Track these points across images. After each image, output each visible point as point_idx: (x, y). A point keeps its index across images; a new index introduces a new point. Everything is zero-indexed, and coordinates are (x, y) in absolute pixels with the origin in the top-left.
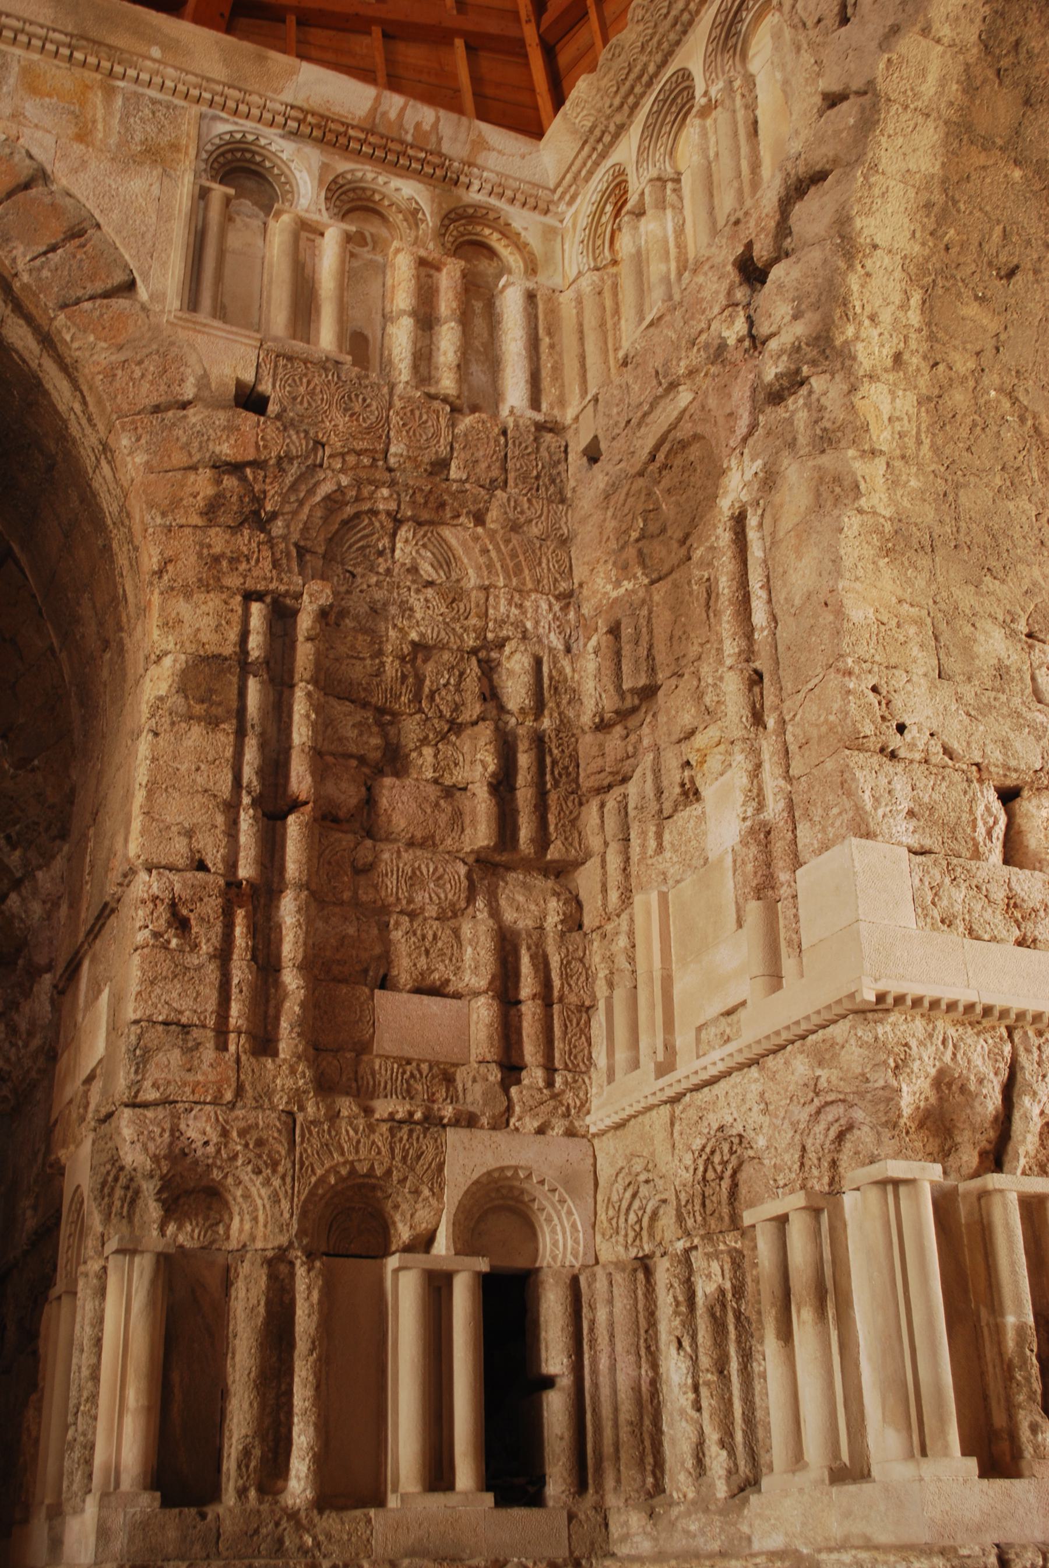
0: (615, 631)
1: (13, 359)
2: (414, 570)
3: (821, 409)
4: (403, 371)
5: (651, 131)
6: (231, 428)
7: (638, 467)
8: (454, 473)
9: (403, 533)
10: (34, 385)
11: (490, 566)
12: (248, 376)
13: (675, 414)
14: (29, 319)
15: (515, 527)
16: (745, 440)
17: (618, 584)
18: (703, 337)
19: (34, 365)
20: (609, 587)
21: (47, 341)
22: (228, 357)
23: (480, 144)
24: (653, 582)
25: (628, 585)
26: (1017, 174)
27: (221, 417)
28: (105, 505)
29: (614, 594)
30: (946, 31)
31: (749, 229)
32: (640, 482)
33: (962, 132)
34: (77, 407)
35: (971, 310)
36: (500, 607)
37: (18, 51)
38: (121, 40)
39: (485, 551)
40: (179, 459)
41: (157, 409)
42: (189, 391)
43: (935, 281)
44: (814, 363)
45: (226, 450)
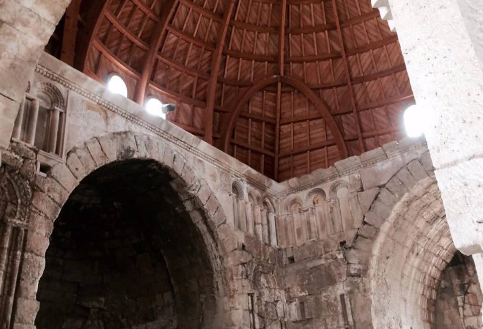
0: (302, 303)
1: (196, 230)
2: (264, 284)
3: (365, 284)
4: (261, 239)
5: (310, 194)
6: (242, 255)
7: (307, 269)
8: (270, 262)
9: (262, 276)
10: (198, 236)
11: (275, 283)
12: (243, 242)
13: (320, 264)
14: (208, 226)
15: (278, 274)
16: (344, 281)
17: (301, 293)
18: (331, 253)
19: (202, 233)
20: (298, 292)
21: (211, 232)
22: (242, 240)
23: (271, 184)
24: (309, 295)
25: (303, 294)
26: (391, 241)
27: (241, 252)
28: (214, 267)
29: (301, 295)
30: (390, 221)
31: (345, 239)
32: (307, 273)
33: (388, 235)
34: (213, 245)
35: (383, 265)
36: (277, 293)
37: (206, 161)
38: (222, 160)
39: (274, 280)
40: (237, 263)
41: (233, 251)
42: (236, 247)
43: (379, 260)
44: (364, 275)
45: (243, 260)
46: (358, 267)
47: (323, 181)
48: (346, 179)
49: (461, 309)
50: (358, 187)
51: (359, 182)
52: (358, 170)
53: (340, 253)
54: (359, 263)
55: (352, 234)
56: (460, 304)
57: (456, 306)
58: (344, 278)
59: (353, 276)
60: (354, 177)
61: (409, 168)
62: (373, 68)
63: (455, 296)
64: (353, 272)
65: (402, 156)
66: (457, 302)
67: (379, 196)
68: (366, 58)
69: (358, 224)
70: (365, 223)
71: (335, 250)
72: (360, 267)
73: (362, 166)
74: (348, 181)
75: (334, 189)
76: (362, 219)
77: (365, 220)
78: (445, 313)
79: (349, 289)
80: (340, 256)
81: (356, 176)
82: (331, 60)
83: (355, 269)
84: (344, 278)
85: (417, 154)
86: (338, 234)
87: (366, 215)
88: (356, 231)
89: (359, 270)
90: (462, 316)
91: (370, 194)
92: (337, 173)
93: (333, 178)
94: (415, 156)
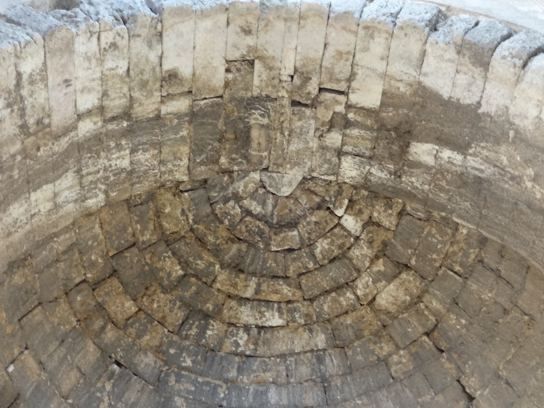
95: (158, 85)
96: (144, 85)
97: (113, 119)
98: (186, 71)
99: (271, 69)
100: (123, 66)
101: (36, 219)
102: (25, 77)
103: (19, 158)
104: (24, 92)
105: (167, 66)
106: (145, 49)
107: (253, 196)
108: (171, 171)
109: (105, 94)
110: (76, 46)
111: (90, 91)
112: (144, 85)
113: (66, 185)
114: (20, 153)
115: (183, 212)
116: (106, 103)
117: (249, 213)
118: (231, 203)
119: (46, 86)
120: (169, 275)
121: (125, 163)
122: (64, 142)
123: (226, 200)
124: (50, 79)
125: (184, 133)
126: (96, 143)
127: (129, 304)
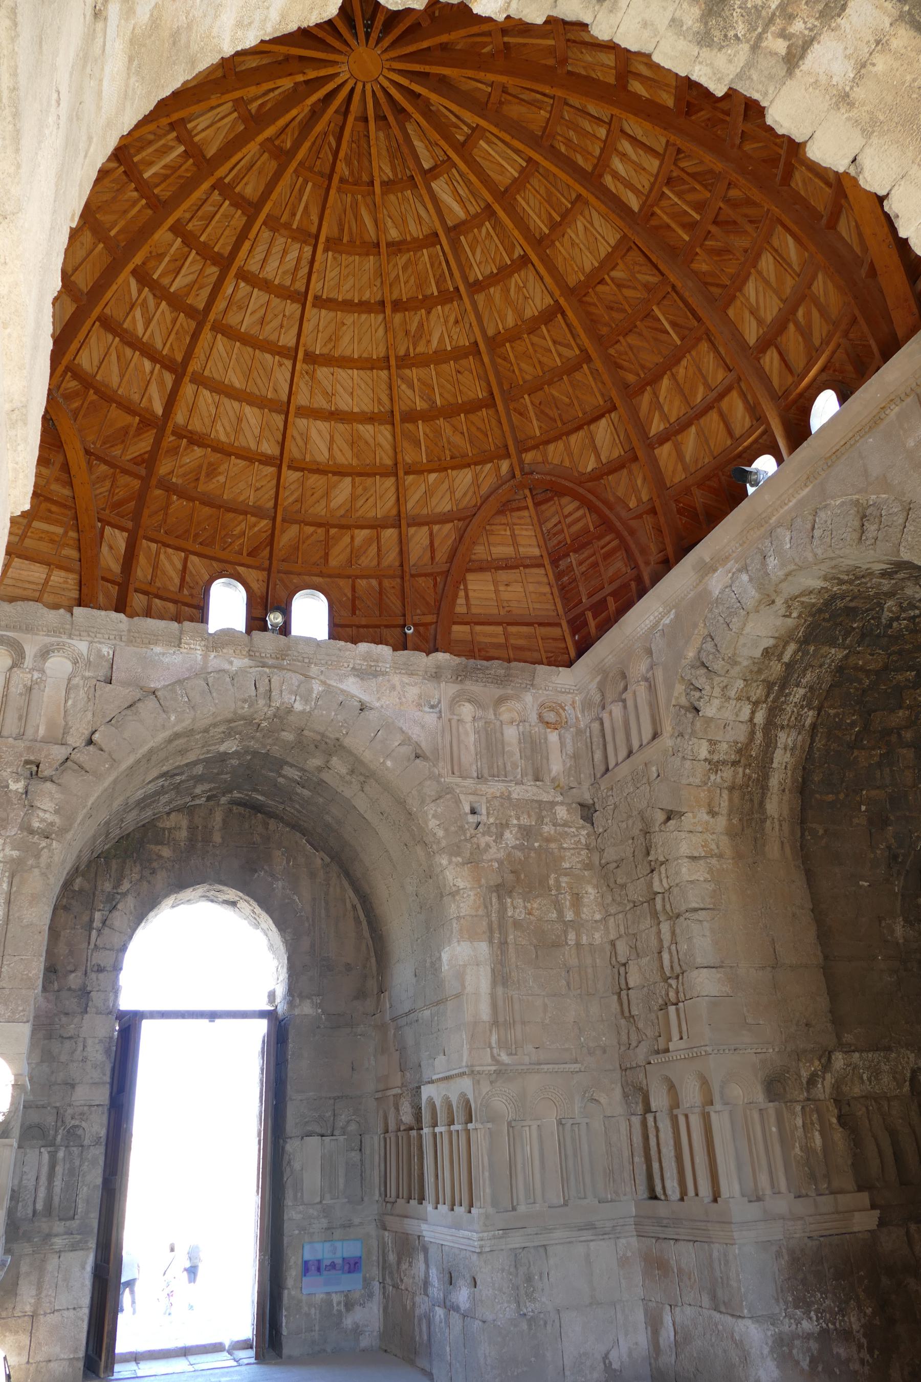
31: (41, 757)
46: (49, 817)
47: (29, 629)
48: (82, 646)
49: (94, 933)
50: (102, 673)
51: (106, 665)
52: (114, 642)
53: (17, 781)
54: (57, 812)
55: (59, 753)
56: (97, 924)
57: (89, 926)
58: (13, 831)
59: (32, 832)
60: (99, 651)
61: (210, 680)
62: (197, 479)
63: (92, 910)
64: (36, 824)
65: (205, 657)
66: (92, 921)
67: (140, 705)
68: (194, 456)
69: (76, 739)
70: (90, 742)
71: (9, 770)
72: (57, 819)
73: (124, 638)
74: (85, 653)
75: (45, 654)
76: (87, 733)
77: (96, 737)
78: (62, 933)
79: (15, 853)
80: (17, 786)
81: (106, 650)
82: (137, 419)
83: (42, 820)
84: (13, 831)
85: (231, 663)
86: (28, 744)
87: (102, 728)
88: (70, 750)
89: (52, 824)
90: (92, 946)
91: (119, 694)
92: (68, 626)
93: (55, 632)
94: (226, 666)
95: (767, 662)
96: (760, 671)
97: (767, 696)
98: (771, 642)
99: (811, 592)
100: (740, 684)
101: (788, 766)
102: (708, 757)
103: (748, 771)
104: (716, 758)
105: (758, 653)
106: (737, 669)
107: (903, 610)
108: (833, 661)
109: (748, 699)
110: (710, 715)
111: (740, 710)
112: (760, 671)
113: (784, 738)
114: (745, 769)
115: (872, 655)
116: (754, 699)
117: (914, 617)
118: (895, 624)
119: (720, 742)
120: (907, 680)
121: (801, 691)
122: (759, 735)
123: (890, 626)
124: (718, 738)
125: (813, 648)
126: (774, 712)
127: (901, 713)
